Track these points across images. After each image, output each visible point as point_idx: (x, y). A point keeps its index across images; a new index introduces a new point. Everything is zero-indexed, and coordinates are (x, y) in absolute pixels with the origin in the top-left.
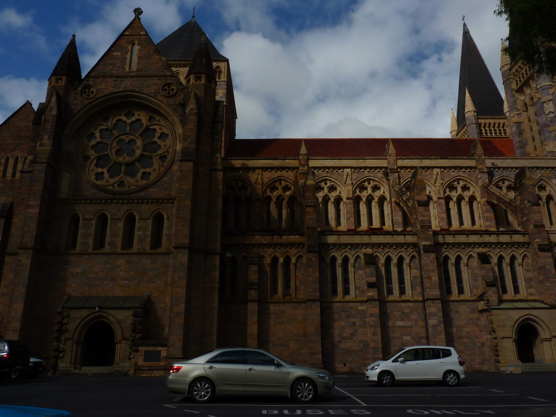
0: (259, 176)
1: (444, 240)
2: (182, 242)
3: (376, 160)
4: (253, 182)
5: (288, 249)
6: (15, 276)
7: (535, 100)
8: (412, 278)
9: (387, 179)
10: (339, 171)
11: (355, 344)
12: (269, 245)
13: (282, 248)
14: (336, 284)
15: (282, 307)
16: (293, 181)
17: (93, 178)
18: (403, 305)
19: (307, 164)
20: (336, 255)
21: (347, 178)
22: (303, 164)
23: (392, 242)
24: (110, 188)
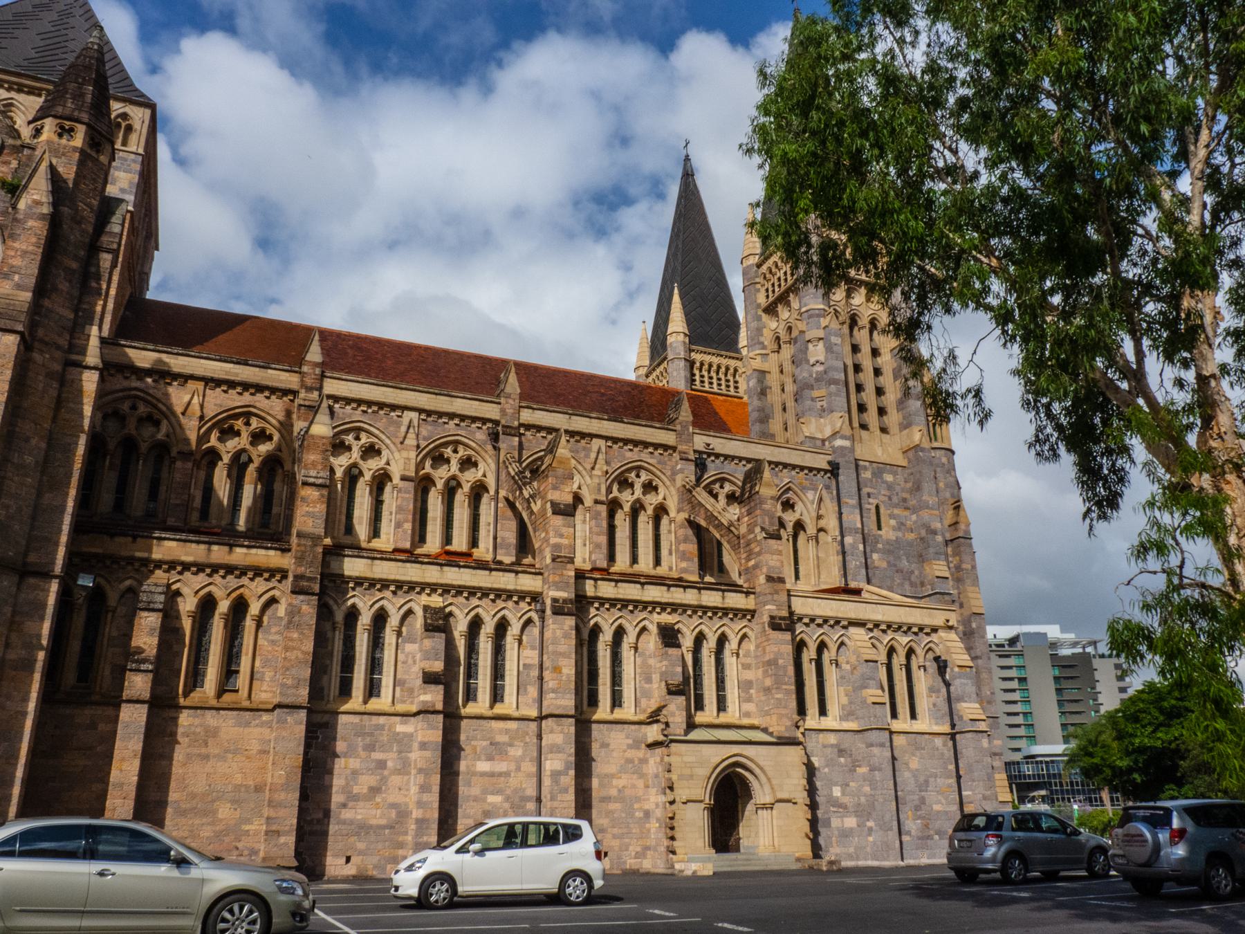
0: (196, 397)
1: (596, 591)
3: (477, 403)
4: (179, 409)
5: (245, 580)
7: (795, 333)
8: (521, 669)
9: (495, 448)
10: (392, 414)
11: (379, 811)
12: (200, 568)
13: (230, 577)
14: (352, 672)
15: (211, 719)
16: (279, 422)
18: (494, 724)
19: (318, 386)
20: (360, 605)
21: (407, 432)
22: (309, 385)
23: (489, 586)
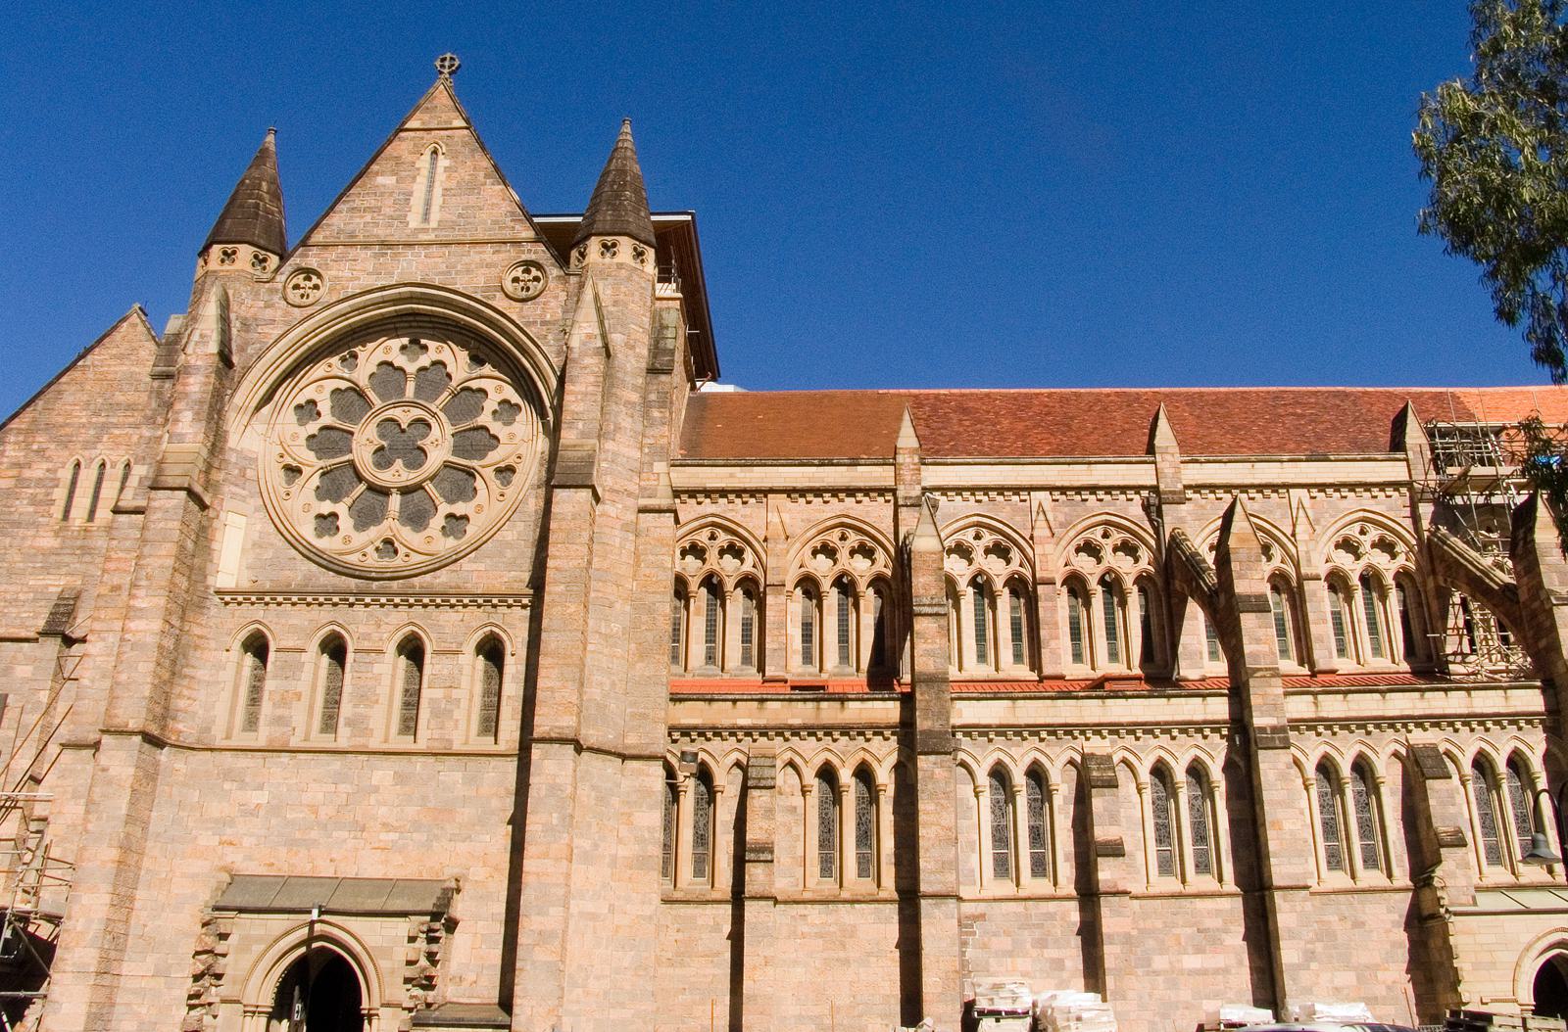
1: (1317, 711)
2: (557, 724)
6: (87, 812)
12: (811, 730)
17: (307, 530)
24: (354, 559)
